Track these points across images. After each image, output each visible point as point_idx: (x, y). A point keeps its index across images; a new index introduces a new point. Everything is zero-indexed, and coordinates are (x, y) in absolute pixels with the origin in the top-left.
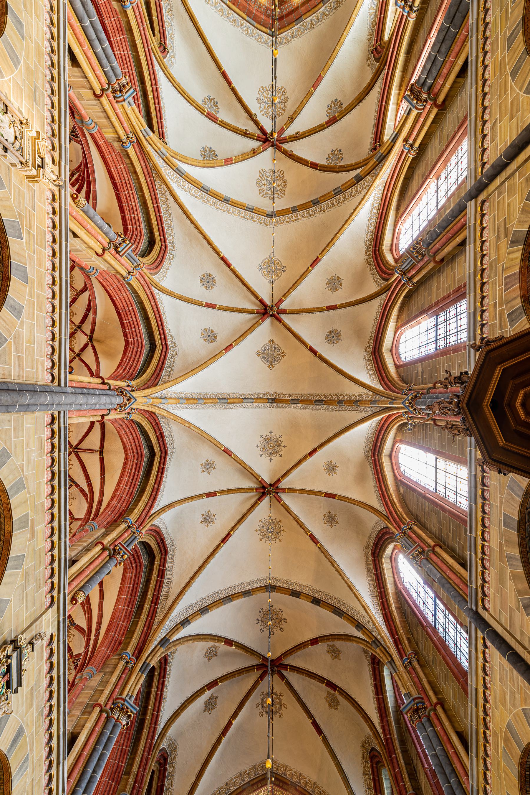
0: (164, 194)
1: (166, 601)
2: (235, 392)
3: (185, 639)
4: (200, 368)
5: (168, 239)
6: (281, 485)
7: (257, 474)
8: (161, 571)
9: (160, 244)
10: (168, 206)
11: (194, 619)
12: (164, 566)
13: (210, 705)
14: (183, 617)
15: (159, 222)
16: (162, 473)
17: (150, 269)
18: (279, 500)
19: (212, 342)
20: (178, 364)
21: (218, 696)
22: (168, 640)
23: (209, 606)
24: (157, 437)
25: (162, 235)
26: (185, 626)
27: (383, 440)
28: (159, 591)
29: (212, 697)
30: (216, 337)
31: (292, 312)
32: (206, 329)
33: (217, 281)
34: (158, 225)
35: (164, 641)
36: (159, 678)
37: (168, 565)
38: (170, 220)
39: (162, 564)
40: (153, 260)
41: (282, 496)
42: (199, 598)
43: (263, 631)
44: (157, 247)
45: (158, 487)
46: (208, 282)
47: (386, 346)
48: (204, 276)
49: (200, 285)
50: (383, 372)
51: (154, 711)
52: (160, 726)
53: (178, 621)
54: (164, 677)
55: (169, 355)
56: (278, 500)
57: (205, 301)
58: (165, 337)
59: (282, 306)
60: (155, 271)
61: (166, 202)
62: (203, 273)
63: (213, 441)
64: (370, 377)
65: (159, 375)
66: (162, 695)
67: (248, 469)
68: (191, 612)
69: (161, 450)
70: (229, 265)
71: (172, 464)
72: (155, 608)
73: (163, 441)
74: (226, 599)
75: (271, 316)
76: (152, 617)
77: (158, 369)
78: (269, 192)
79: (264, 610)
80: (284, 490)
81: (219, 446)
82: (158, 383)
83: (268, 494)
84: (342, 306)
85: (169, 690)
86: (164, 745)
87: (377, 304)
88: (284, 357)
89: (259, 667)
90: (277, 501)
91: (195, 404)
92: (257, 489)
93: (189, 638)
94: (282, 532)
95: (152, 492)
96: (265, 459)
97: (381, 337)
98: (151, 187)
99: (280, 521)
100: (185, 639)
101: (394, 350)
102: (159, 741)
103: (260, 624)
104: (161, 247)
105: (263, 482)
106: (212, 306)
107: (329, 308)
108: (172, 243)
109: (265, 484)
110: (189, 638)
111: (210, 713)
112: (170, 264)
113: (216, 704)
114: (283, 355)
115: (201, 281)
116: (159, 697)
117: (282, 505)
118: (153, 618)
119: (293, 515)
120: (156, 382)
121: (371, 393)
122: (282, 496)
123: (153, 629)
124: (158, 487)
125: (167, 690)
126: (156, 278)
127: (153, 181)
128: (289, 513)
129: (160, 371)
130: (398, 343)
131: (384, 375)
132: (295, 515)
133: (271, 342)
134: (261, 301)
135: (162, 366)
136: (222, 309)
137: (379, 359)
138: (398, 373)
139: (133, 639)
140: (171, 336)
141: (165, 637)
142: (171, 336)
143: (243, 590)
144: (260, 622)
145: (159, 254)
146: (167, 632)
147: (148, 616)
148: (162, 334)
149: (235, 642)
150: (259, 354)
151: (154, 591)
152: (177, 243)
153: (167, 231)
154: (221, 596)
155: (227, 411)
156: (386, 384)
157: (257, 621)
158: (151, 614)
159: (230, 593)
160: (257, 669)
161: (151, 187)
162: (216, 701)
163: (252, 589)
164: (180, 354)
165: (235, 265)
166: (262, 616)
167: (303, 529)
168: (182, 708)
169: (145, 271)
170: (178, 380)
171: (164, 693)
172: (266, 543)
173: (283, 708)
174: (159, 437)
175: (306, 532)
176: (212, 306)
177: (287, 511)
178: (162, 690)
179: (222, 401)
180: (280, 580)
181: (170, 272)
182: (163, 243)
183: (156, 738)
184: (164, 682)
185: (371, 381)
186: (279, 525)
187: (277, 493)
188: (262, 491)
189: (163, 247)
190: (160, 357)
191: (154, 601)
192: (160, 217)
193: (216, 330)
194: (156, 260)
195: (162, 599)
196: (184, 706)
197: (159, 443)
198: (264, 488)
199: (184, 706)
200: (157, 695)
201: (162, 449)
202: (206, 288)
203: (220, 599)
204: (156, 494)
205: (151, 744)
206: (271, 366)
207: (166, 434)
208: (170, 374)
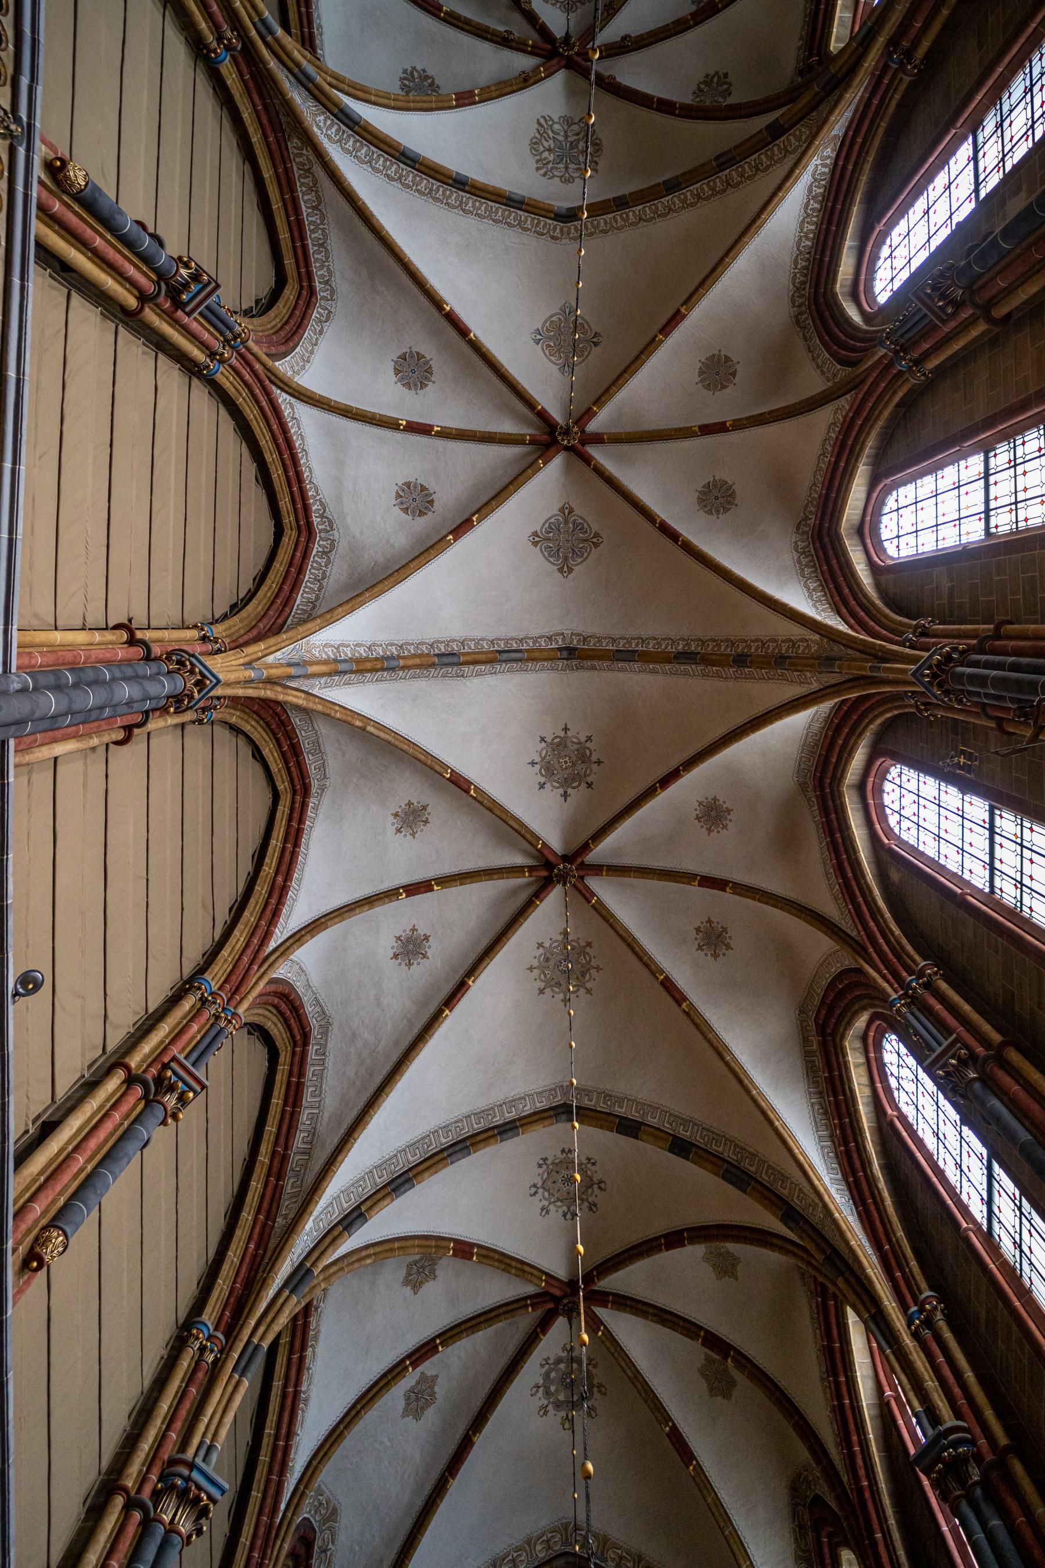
0: (308, 171)
1: (305, 1166)
2: (477, 634)
3: (355, 1258)
4: (392, 579)
5: (318, 274)
6: (591, 858)
7: (532, 834)
8: (293, 1088)
9: (297, 286)
10: (318, 197)
11: (376, 1209)
12: (301, 1074)
13: (417, 1400)
14: (347, 1206)
15: (296, 234)
16: (296, 844)
17: (270, 343)
18: (587, 895)
19: (421, 514)
20: (338, 572)
21: (437, 1376)
22: (309, 1271)
23: (415, 1171)
24: (283, 755)
25: (302, 264)
26: (353, 1230)
27: (847, 755)
28: (287, 1140)
29: (423, 1377)
30: (431, 502)
31: (617, 439)
32: (408, 484)
33: (435, 368)
34: (293, 242)
35: (300, 1275)
36: (291, 1352)
37: (310, 1070)
38: (323, 230)
39: (296, 1070)
40: (277, 322)
41: (594, 883)
42: (388, 1151)
43: (548, 1212)
44: (289, 293)
45: (285, 881)
46: (413, 371)
47: (847, 521)
48: (403, 357)
49: (394, 379)
50: (843, 584)
51: (277, 1438)
52: (292, 1475)
53: (336, 1216)
54: (303, 1347)
55: (316, 549)
56: (584, 896)
57: (404, 417)
58: (306, 508)
59: (593, 426)
60: (283, 348)
61: (314, 187)
62: (400, 353)
63: (422, 757)
64: (811, 596)
65: (289, 601)
66: (296, 1394)
67: (512, 823)
68: (369, 1190)
69: (293, 786)
70: (462, 331)
71: (321, 817)
72: (276, 1185)
73: (300, 766)
74: (457, 1148)
75: (567, 448)
76: (269, 1212)
77: (286, 588)
78: (560, 166)
79: (549, 1162)
80: (597, 869)
81: (438, 768)
82: (285, 622)
83: (559, 882)
84: (739, 425)
85: (316, 1378)
86: (305, 1512)
87: (825, 419)
88: (596, 545)
89: (536, 1299)
90: (581, 899)
91: (377, 670)
92: (531, 868)
93: (364, 1253)
94: (593, 971)
95: (270, 896)
96: (552, 796)
97: (836, 498)
98: (277, 155)
99: (589, 944)
100: (355, 1258)
101: (866, 530)
102: (289, 1515)
103: (539, 1196)
104: (300, 294)
105: (546, 852)
106: (422, 429)
107: (707, 430)
108: (327, 282)
109: (551, 858)
110: (364, 1253)
111: (417, 1418)
112: (321, 332)
113: (433, 1394)
114: (595, 539)
115: (397, 372)
116: (289, 1401)
117: (593, 906)
118: (273, 1214)
119: (621, 932)
120: (280, 621)
121: (817, 637)
122: (594, 883)
123: (271, 1245)
124: (285, 881)
125: (310, 1378)
126: (283, 366)
127: (281, 139)
128: (611, 926)
129: (291, 591)
130: (878, 514)
131: (846, 591)
132: (627, 930)
133: (566, 511)
134: (542, 416)
135: (297, 579)
136: (447, 434)
137: (831, 553)
138: (878, 585)
139: (220, 1281)
140: (322, 504)
141: (301, 1264)
142: (322, 504)
143: (498, 1120)
144: (541, 1191)
145: (295, 308)
146: (307, 1249)
147: (258, 1212)
148: (298, 499)
149: (479, 1246)
150: (536, 539)
151: (276, 1143)
152: (341, 285)
153: (315, 256)
154: (444, 1141)
155: (459, 683)
156: (853, 614)
157: (533, 1190)
158: (265, 1205)
159: (466, 1131)
160: (532, 1305)
161: (277, 155)
162: (432, 1388)
163: (520, 1119)
164: (342, 547)
165: (478, 330)
166: (545, 1175)
167: (647, 966)
168: (348, 1419)
169: (256, 349)
170: (336, 612)
171: (304, 1388)
172: (553, 999)
173: (596, 1395)
174: (289, 755)
175: (653, 974)
176: (422, 429)
177: (607, 921)
178: (298, 1383)
179: (445, 660)
180: (589, 1091)
181: (320, 351)
182: (305, 284)
183: (283, 1506)
184: (302, 1359)
185: (814, 606)
186: (585, 954)
187: (582, 878)
188: (545, 873)
189: (304, 292)
190: (293, 556)
191: (275, 1170)
192: (300, 223)
193: (431, 484)
194: (286, 323)
195: (294, 1158)
196: (354, 1413)
197: (288, 769)
198: (548, 865)
199: (354, 1413)
200: (284, 1395)
201: (296, 781)
202: (408, 385)
203: (442, 1151)
204: (280, 902)
205: (270, 1526)
206: (565, 569)
207: (305, 746)
208: (317, 598)
